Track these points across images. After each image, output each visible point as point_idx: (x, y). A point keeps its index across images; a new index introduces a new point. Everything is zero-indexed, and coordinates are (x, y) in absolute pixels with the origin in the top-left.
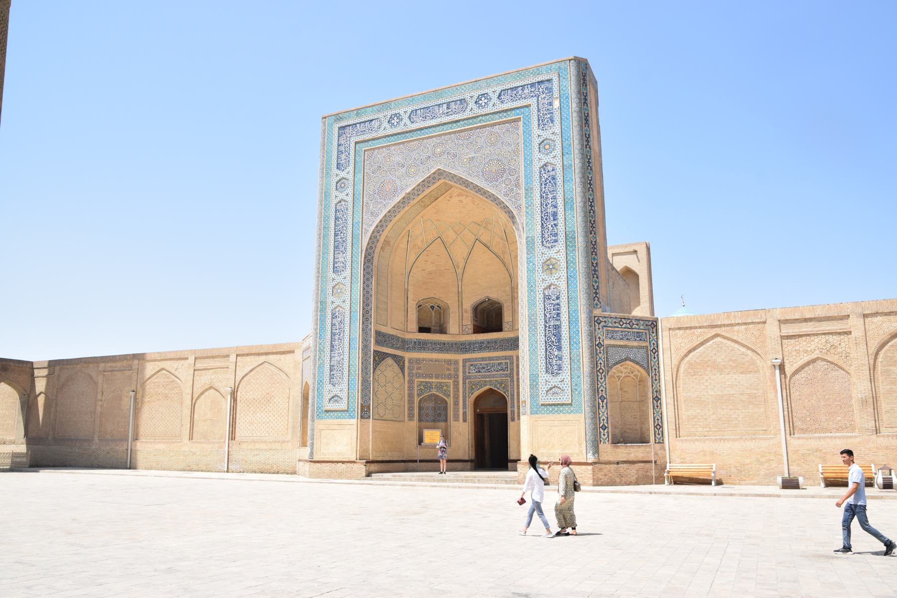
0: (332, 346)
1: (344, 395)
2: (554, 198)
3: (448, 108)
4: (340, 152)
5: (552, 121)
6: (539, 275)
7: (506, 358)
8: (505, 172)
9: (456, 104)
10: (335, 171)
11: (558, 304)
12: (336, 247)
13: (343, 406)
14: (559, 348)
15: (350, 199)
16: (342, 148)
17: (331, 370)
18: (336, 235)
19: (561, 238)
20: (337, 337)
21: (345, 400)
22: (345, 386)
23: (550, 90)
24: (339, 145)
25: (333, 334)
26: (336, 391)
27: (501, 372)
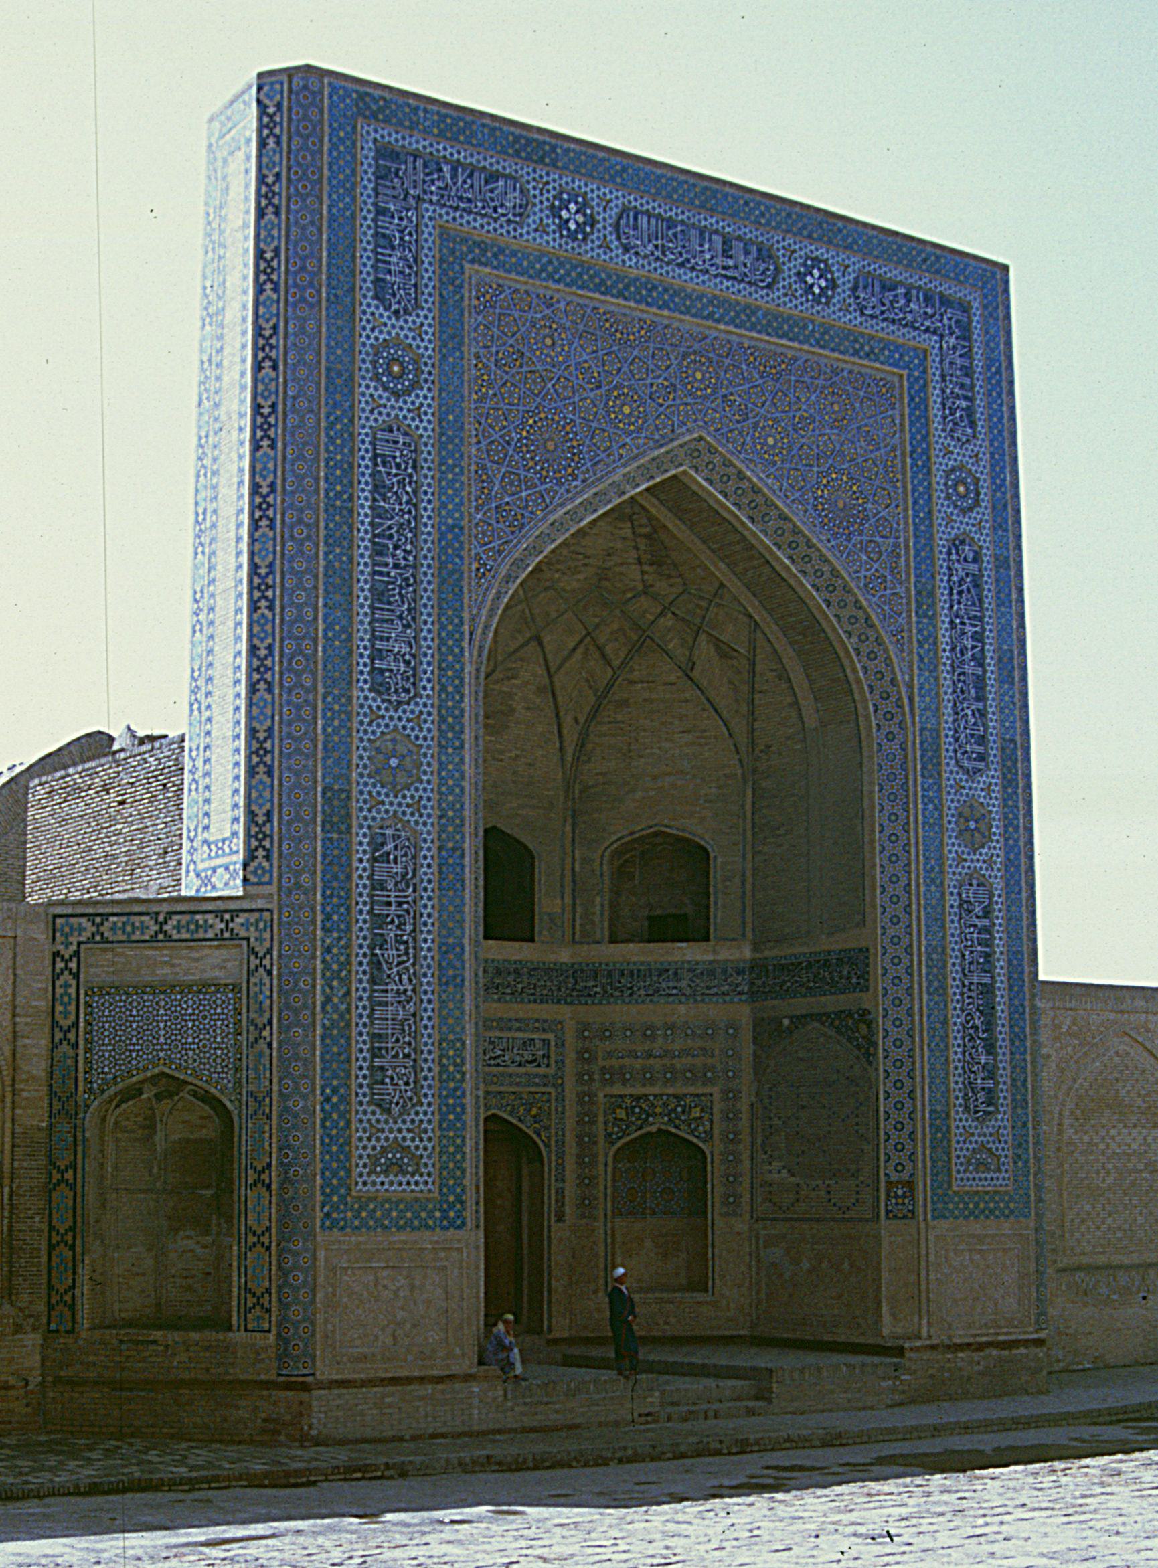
0: (376, 964)
1: (426, 1148)
2: (978, 638)
3: (726, 254)
4: (383, 240)
5: (972, 424)
6: (952, 847)
7: (545, 1025)
8: (867, 518)
9: (747, 253)
10: (367, 303)
11: (987, 930)
12: (379, 595)
13: (423, 1185)
14: (990, 1049)
15: (425, 429)
16: (390, 227)
17: (375, 1053)
18: (379, 551)
19: (993, 752)
20: (391, 933)
21: (430, 1164)
22: (427, 1113)
23: (966, 336)
24: (380, 212)
25: (379, 921)
26: (396, 1130)
27: (531, 1069)
